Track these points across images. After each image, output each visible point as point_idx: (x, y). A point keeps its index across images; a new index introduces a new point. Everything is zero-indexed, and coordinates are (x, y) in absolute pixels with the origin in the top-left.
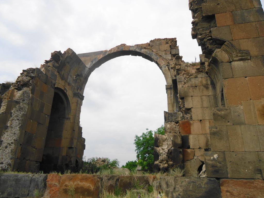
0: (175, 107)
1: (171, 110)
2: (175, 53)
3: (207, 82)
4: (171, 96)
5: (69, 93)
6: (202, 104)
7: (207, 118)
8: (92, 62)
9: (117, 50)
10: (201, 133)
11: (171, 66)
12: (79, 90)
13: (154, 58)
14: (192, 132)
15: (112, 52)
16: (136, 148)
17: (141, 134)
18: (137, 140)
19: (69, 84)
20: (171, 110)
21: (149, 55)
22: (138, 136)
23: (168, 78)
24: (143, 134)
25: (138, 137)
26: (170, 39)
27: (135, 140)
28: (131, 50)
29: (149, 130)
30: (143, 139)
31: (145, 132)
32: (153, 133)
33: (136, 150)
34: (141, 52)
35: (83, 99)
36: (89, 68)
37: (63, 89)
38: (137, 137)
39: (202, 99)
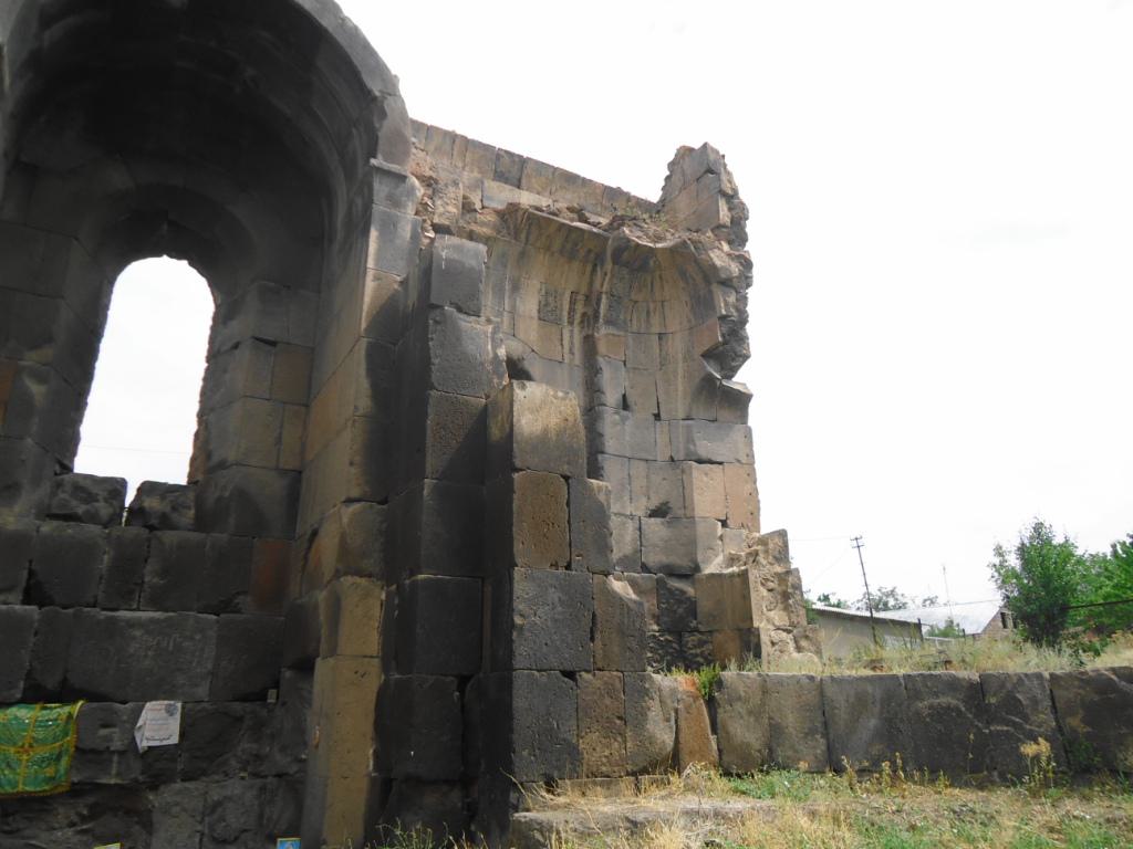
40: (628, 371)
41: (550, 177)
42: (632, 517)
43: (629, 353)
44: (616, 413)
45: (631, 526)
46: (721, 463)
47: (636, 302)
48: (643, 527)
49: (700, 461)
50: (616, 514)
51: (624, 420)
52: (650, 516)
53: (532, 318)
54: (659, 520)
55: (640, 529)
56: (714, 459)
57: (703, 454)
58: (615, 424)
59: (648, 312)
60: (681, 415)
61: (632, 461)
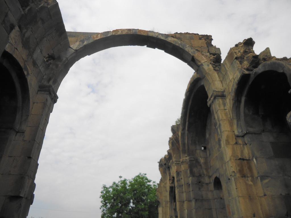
0: (235, 126)
1: (228, 131)
2: (214, 52)
4: (225, 108)
5: (32, 81)
8: (83, 41)
9: (127, 33)
11: (237, 55)
12: (51, 83)
13: (189, 51)
15: (119, 33)
16: (101, 204)
17: (111, 184)
18: (104, 192)
19: (35, 64)
20: (229, 130)
21: (181, 46)
22: (106, 187)
23: (216, 81)
24: (114, 183)
25: (107, 188)
26: (203, 36)
27: (102, 192)
28: (151, 36)
29: (123, 179)
30: (114, 190)
31: (117, 180)
32: (128, 182)
33: (102, 206)
34: (167, 41)
35: (55, 102)
36: (76, 50)
37: (22, 65)
38: (104, 187)
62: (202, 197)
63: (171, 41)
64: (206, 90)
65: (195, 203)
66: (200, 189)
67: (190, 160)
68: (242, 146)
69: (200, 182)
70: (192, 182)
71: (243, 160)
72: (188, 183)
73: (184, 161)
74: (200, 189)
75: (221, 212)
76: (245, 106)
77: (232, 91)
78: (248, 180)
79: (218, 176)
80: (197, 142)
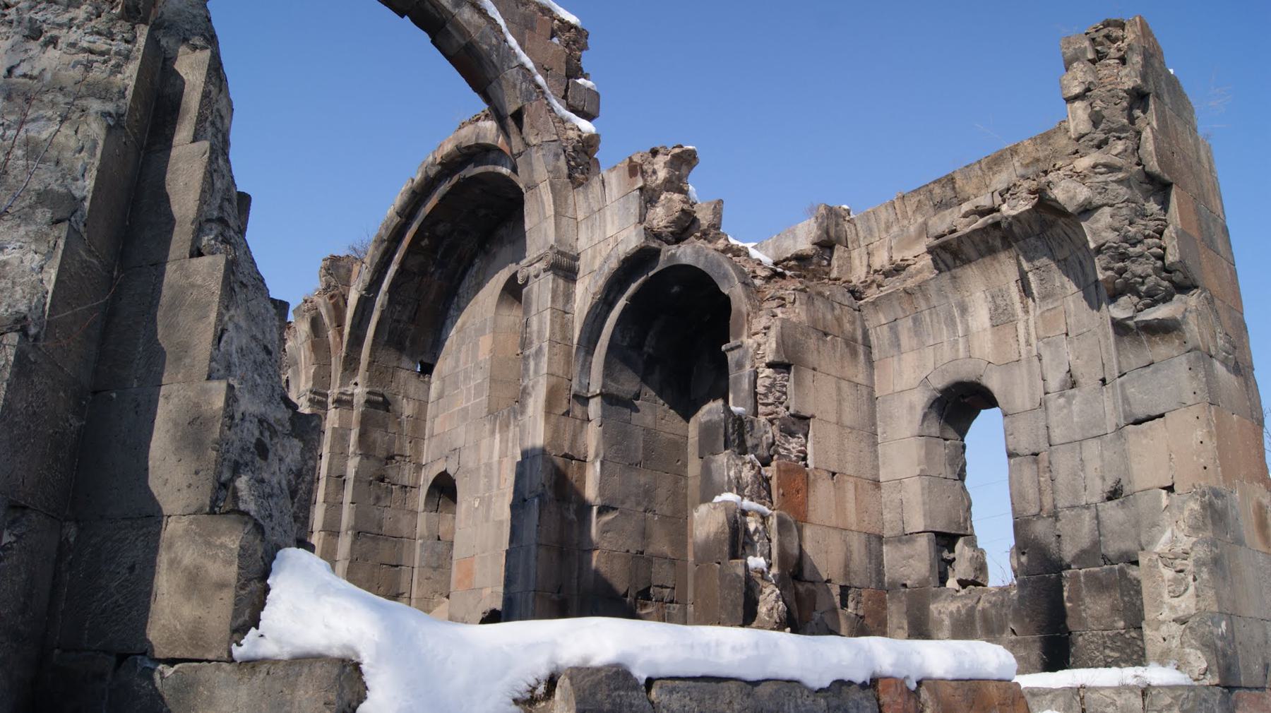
3: (854, 330)
6: (839, 413)
7: (850, 469)
10: (834, 523)
14: (812, 517)
39: (839, 389)
40: (1071, 342)
41: (980, 173)
42: (1087, 506)
43: (1071, 321)
44: (1061, 396)
45: (1087, 516)
46: (1162, 416)
47: (1065, 260)
48: (1101, 514)
49: (1138, 422)
50: (1068, 508)
51: (1069, 401)
52: (1109, 499)
53: (985, 330)
54: (1113, 503)
55: (1097, 517)
56: (1153, 414)
57: (1140, 413)
58: (1061, 408)
59: (1081, 263)
60: (1117, 374)
61: (1084, 443)
62: (381, 528)
63: (470, 24)
64: (527, 228)
65: (353, 543)
66: (378, 499)
67: (367, 402)
68: (578, 422)
69: (382, 480)
70: (357, 473)
71: (572, 458)
72: (340, 476)
73: (344, 397)
74: (378, 499)
75: (428, 579)
76: (617, 325)
77: (600, 269)
78: (568, 509)
79: (451, 472)
80: (408, 343)
